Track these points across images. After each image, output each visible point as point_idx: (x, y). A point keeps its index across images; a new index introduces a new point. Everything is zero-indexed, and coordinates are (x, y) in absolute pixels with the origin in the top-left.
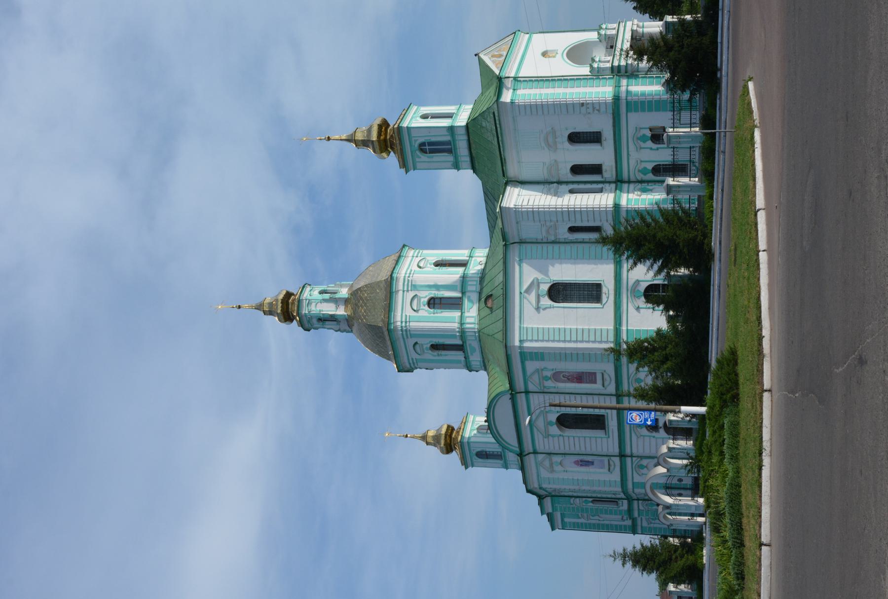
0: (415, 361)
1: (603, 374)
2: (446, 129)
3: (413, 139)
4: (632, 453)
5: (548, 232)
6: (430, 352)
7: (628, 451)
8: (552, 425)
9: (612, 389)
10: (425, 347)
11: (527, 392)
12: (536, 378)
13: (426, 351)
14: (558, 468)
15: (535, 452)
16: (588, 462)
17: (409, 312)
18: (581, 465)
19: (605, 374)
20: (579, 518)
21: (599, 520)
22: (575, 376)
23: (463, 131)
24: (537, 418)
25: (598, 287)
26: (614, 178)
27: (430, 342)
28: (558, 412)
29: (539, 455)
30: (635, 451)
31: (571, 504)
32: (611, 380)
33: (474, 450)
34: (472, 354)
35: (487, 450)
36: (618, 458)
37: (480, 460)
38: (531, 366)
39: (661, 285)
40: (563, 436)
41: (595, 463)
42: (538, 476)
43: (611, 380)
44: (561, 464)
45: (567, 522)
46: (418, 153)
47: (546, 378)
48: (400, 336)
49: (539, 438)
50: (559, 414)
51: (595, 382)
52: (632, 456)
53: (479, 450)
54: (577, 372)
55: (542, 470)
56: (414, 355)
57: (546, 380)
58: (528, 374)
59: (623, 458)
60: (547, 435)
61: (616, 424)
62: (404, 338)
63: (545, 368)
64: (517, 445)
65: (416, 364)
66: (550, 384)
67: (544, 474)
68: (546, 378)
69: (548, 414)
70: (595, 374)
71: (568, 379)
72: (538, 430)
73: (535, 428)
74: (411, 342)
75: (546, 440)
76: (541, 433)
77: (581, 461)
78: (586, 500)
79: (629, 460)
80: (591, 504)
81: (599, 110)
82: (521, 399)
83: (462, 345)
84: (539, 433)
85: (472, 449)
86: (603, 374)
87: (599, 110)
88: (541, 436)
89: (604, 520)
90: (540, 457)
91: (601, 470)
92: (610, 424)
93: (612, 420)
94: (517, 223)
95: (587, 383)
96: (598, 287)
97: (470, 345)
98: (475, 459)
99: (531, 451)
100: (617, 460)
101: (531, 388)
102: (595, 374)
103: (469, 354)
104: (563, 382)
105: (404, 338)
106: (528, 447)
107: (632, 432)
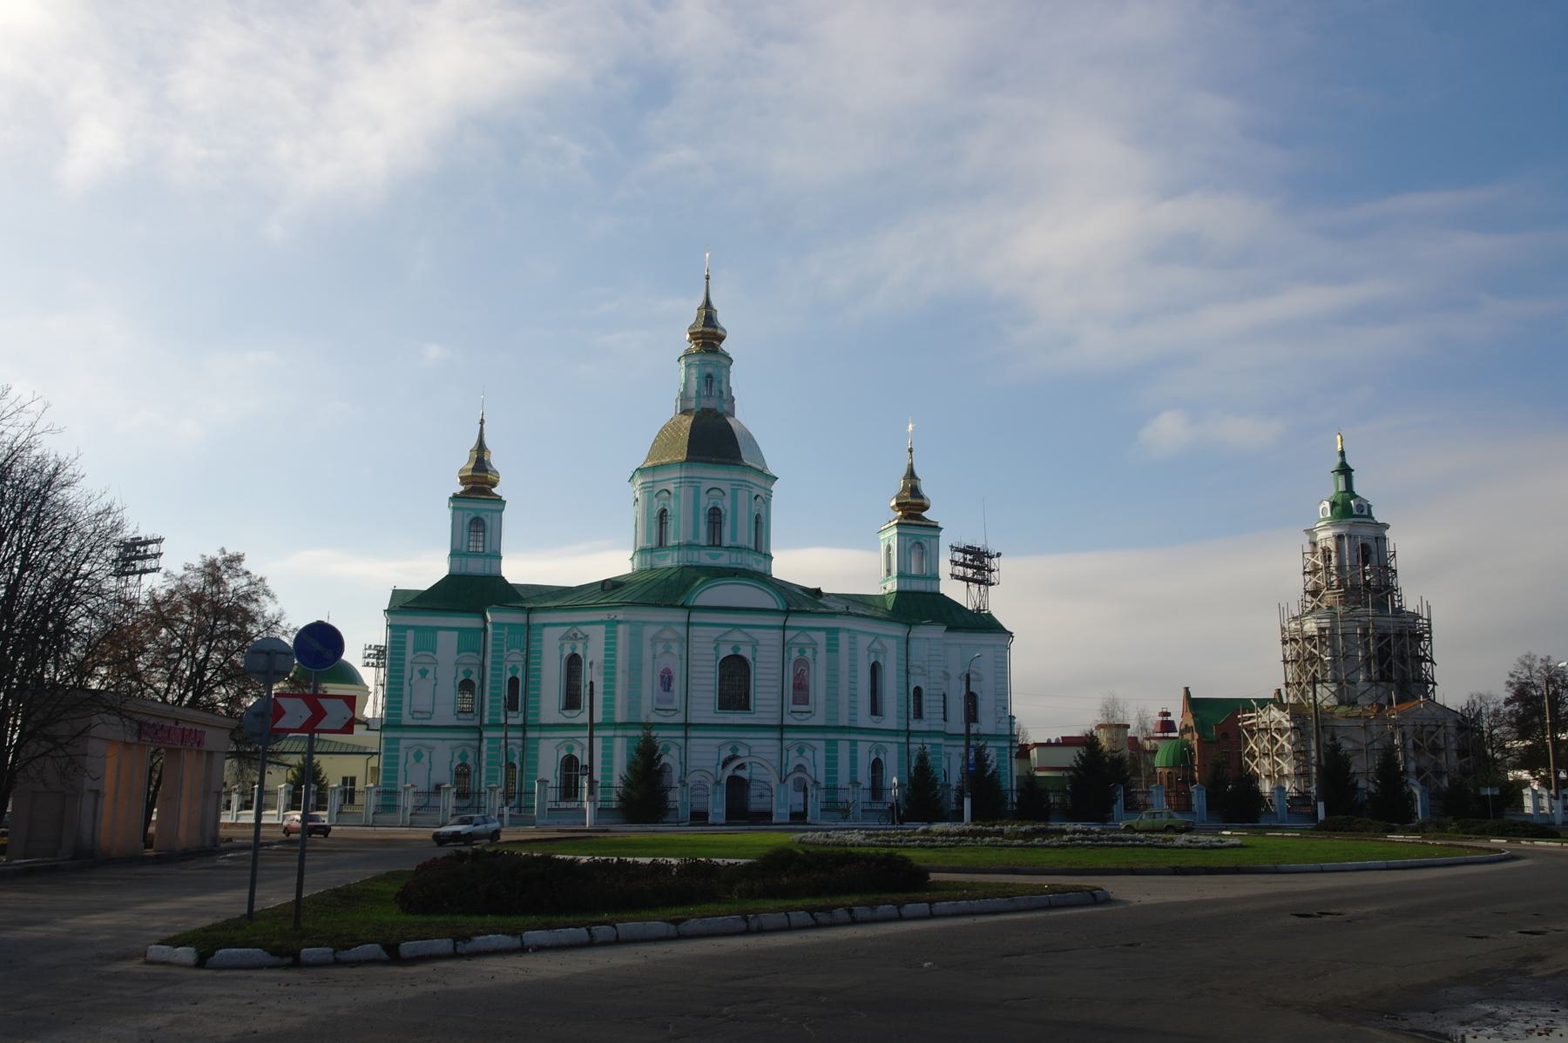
0: (695, 485)
1: (810, 712)
2: (936, 572)
3: (928, 539)
4: (691, 738)
5: (919, 667)
6: (711, 506)
7: (692, 734)
8: (733, 648)
9: (788, 720)
10: (719, 502)
11: (784, 628)
12: (802, 639)
13: (712, 501)
14: (660, 648)
15: (689, 624)
16: (669, 685)
17: (755, 492)
18: (662, 677)
19: (809, 714)
20: (415, 651)
21: (410, 680)
22: (803, 683)
23: (934, 589)
24: (746, 634)
25: (744, 705)
26: (910, 728)
27: (726, 510)
28: (754, 659)
29: (685, 629)
30: (691, 742)
31: (508, 650)
32: (801, 720)
33: (487, 516)
34: (707, 554)
35: (488, 534)
36: (683, 721)
37: (467, 521)
38: (820, 638)
39: (829, 776)
40: (716, 660)
41: (666, 693)
42: (645, 623)
43: (801, 720)
44: (667, 652)
45: (406, 632)
46: (914, 541)
47: (802, 651)
48: (747, 479)
49: (716, 632)
50: (750, 659)
51: (794, 703)
52: (686, 738)
53: (488, 522)
54: (808, 686)
55: (660, 628)
56: (704, 489)
57: (799, 651)
58: (808, 633)
59: (684, 727)
60: (718, 642)
61: (736, 723)
62: (731, 480)
63: (816, 652)
64: (695, 604)
65: (690, 484)
66: (795, 654)
67: (650, 631)
68: (802, 651)
69: (750, 648)
70: (807, 704)
71: (799, 675)
72: (726, 634)
73: (729, 629)
74: (726, 487)
75: (713, 640)
76: (721, 636)
77: (670, 678)
78: (518, 670)
79: (681, 733)
80: (509, 675)
81: (999, 722)
82: (777, 620)
83: (720, 546)
84: (721, 634)
85: (490, 514)
86: (810, 712)
87: (999, 722)
88: (717, 635)
89: (410, 685)
90: (682, 631)
91: (655, 701)
92: (736, 715)
93: (743, 718)
94: (928, 639)
95: (793, 694)
96: (744, 705)
97: (722, 555)
98: (468, 515)
99: (691, 620)
100: (679, 718)
101: (790, 634)
102: (807, 704)
103: (708, 551)
104: (794, 669)
105: (731, 480)
106: (696, 617)
107: (728, 741)
